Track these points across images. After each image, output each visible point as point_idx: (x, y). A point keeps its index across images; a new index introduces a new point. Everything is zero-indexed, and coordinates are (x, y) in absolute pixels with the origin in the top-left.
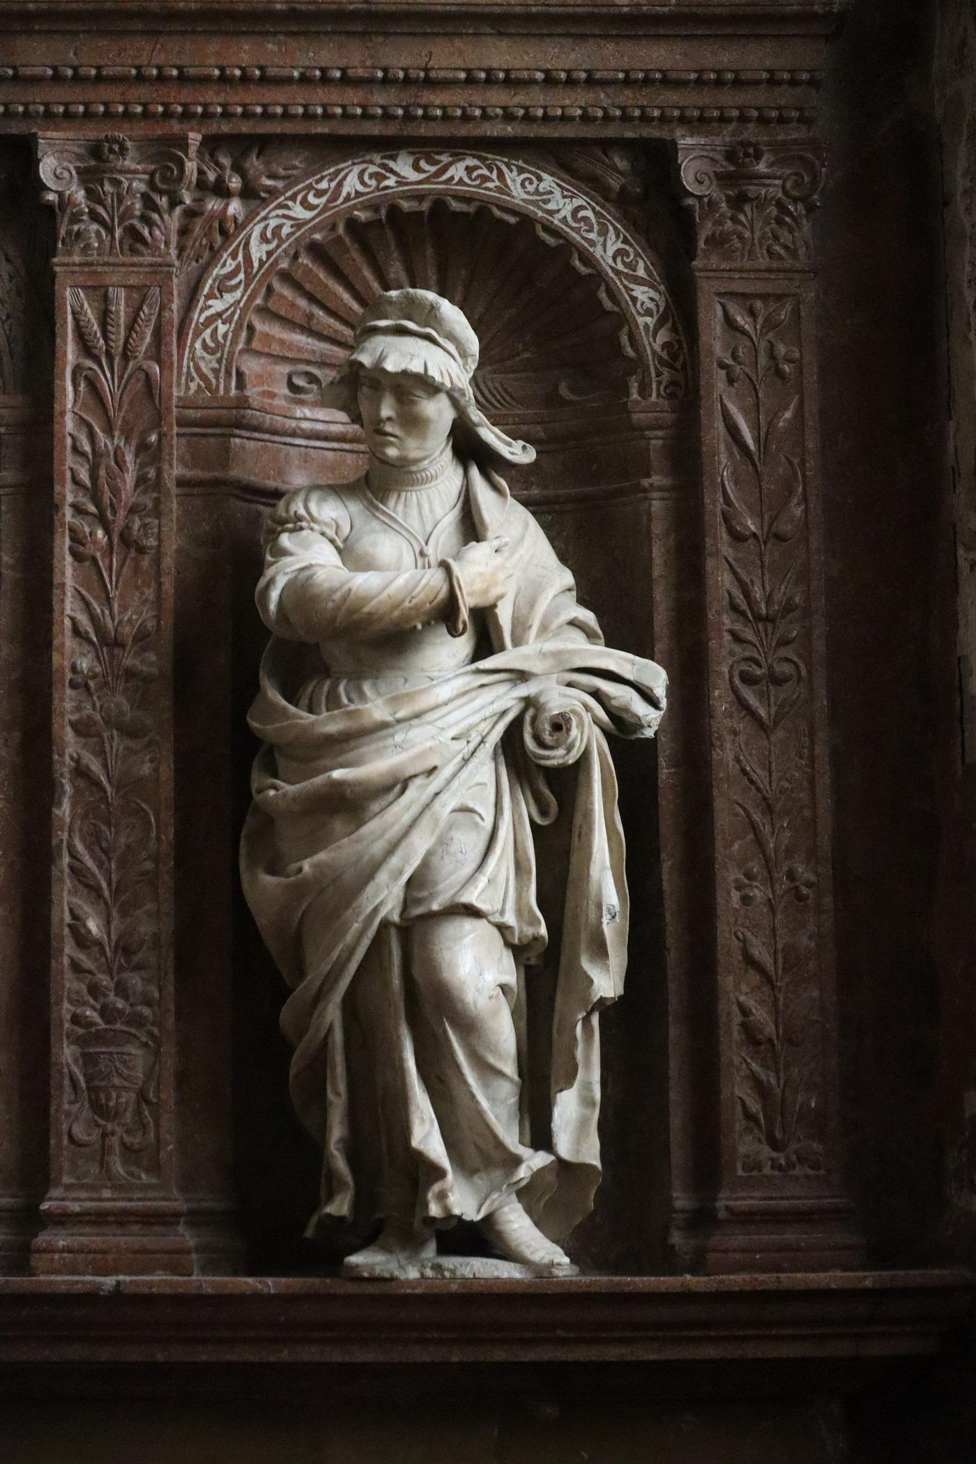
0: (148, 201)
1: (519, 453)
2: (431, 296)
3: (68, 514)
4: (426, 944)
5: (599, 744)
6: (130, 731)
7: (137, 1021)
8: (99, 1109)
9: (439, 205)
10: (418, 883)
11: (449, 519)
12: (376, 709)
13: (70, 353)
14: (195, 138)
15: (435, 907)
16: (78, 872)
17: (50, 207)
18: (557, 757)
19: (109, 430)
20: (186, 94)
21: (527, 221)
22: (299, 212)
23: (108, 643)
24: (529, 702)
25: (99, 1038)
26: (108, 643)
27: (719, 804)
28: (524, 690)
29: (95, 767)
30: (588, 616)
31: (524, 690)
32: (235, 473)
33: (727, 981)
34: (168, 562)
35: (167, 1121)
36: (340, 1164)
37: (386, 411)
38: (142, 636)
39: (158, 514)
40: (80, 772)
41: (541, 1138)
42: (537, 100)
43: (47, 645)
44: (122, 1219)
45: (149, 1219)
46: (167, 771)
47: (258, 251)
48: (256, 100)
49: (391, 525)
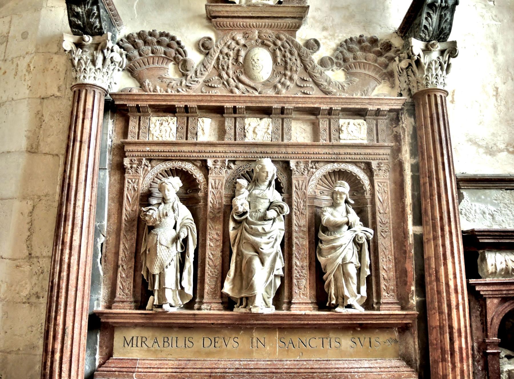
0: (304, 170)
1: (352, 202)
2: (343, 182)
3: (294, 210)
4: (346, 267)
5: (366, 241)
6: (303, 238)
7: (304, 277)
8: (299, 288)
9: (340, 170)
10: (344, 259)
11: (345, 210)
12: (338, 236)
13: (294, 189)
14: (310, 161)
15: (347, 262)
16: (296, 257)
17: (291, 170)
18: (360, 242)
19: (299, 198)
20: (309, 155)
21: (351, 172)
22: (322, 170)
23: (300, 226)
24: (356, 235)
25: (299, 279)
26: (300, 226)
27: (379, 248)
28: (356, 233)
29: (298, 243)
30: (362, 223)
31: (356, 233)
32: (315, 204)
33: (381, 271)
34: (307, 216)
35: (308, 290)
36: (333, 296)
37: (338, 196)
38: (304, 226)
39: (306, 209)
40: (296, 243)
41: (359, 292)
42: (353, 156)
43: (292, 227)
44: (302, 303)
45: (306, 303)
46: (307, 243)
47: (317, 176)
48: (318, 156)
49: (337, 211)
